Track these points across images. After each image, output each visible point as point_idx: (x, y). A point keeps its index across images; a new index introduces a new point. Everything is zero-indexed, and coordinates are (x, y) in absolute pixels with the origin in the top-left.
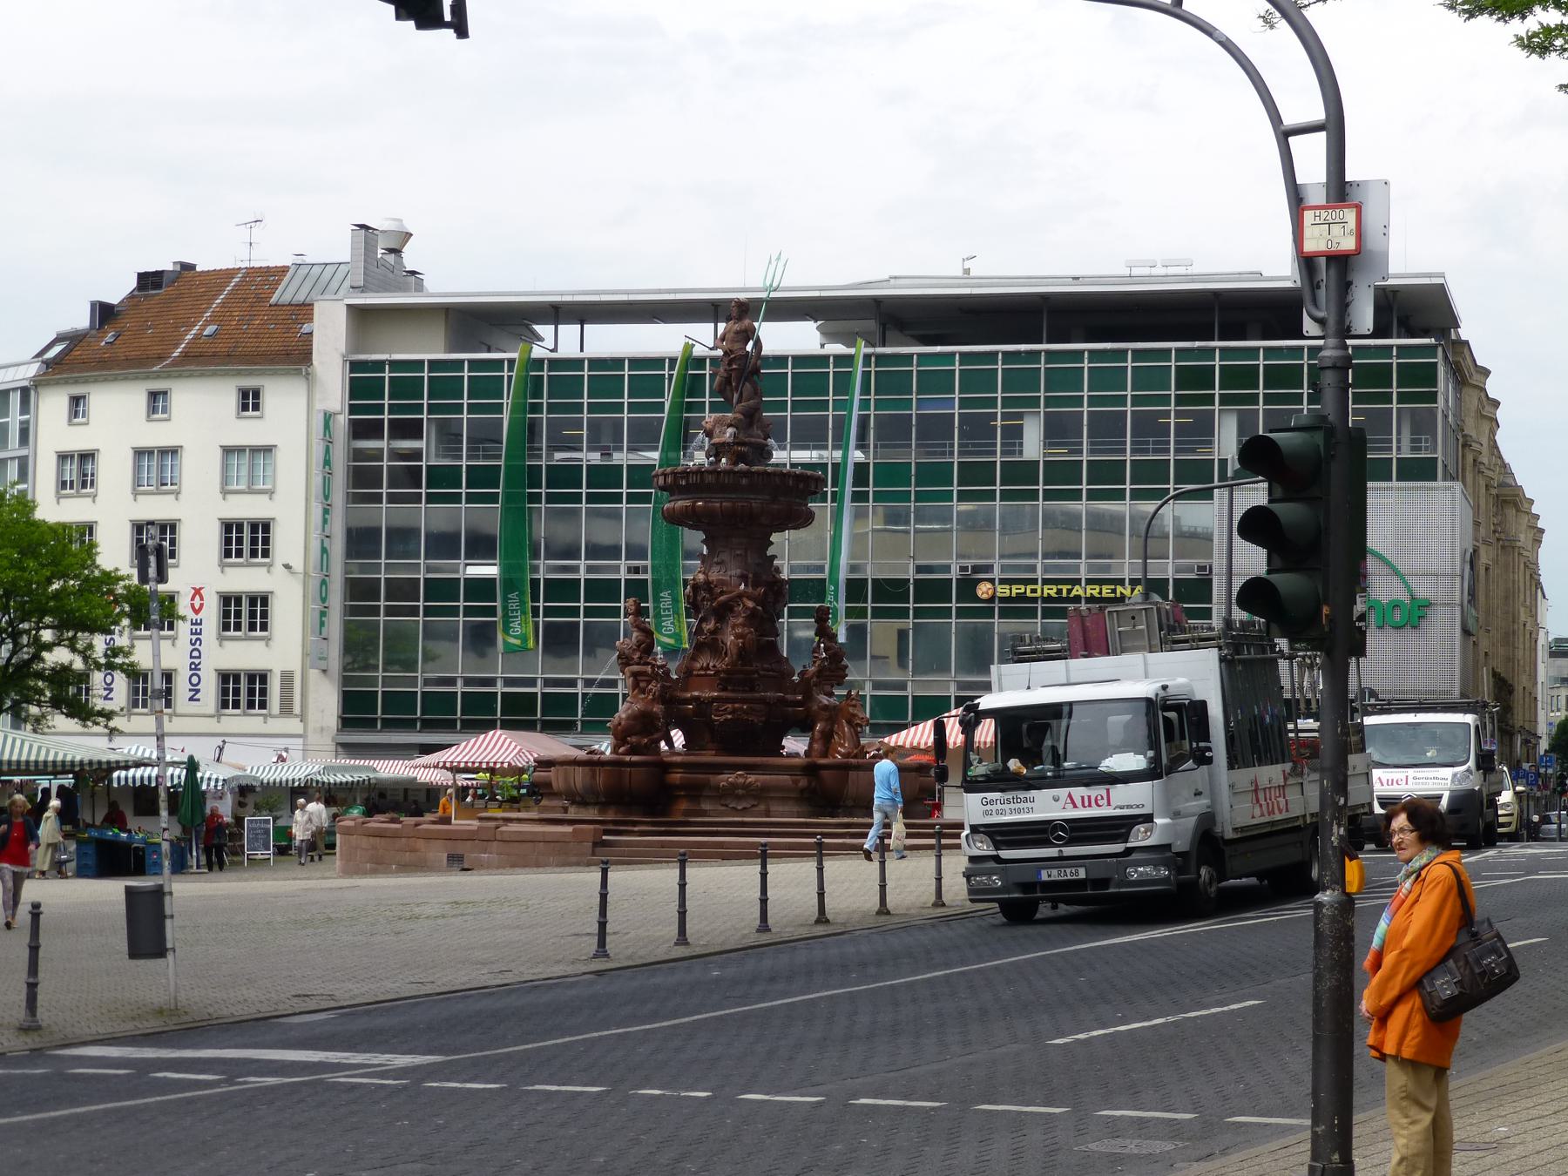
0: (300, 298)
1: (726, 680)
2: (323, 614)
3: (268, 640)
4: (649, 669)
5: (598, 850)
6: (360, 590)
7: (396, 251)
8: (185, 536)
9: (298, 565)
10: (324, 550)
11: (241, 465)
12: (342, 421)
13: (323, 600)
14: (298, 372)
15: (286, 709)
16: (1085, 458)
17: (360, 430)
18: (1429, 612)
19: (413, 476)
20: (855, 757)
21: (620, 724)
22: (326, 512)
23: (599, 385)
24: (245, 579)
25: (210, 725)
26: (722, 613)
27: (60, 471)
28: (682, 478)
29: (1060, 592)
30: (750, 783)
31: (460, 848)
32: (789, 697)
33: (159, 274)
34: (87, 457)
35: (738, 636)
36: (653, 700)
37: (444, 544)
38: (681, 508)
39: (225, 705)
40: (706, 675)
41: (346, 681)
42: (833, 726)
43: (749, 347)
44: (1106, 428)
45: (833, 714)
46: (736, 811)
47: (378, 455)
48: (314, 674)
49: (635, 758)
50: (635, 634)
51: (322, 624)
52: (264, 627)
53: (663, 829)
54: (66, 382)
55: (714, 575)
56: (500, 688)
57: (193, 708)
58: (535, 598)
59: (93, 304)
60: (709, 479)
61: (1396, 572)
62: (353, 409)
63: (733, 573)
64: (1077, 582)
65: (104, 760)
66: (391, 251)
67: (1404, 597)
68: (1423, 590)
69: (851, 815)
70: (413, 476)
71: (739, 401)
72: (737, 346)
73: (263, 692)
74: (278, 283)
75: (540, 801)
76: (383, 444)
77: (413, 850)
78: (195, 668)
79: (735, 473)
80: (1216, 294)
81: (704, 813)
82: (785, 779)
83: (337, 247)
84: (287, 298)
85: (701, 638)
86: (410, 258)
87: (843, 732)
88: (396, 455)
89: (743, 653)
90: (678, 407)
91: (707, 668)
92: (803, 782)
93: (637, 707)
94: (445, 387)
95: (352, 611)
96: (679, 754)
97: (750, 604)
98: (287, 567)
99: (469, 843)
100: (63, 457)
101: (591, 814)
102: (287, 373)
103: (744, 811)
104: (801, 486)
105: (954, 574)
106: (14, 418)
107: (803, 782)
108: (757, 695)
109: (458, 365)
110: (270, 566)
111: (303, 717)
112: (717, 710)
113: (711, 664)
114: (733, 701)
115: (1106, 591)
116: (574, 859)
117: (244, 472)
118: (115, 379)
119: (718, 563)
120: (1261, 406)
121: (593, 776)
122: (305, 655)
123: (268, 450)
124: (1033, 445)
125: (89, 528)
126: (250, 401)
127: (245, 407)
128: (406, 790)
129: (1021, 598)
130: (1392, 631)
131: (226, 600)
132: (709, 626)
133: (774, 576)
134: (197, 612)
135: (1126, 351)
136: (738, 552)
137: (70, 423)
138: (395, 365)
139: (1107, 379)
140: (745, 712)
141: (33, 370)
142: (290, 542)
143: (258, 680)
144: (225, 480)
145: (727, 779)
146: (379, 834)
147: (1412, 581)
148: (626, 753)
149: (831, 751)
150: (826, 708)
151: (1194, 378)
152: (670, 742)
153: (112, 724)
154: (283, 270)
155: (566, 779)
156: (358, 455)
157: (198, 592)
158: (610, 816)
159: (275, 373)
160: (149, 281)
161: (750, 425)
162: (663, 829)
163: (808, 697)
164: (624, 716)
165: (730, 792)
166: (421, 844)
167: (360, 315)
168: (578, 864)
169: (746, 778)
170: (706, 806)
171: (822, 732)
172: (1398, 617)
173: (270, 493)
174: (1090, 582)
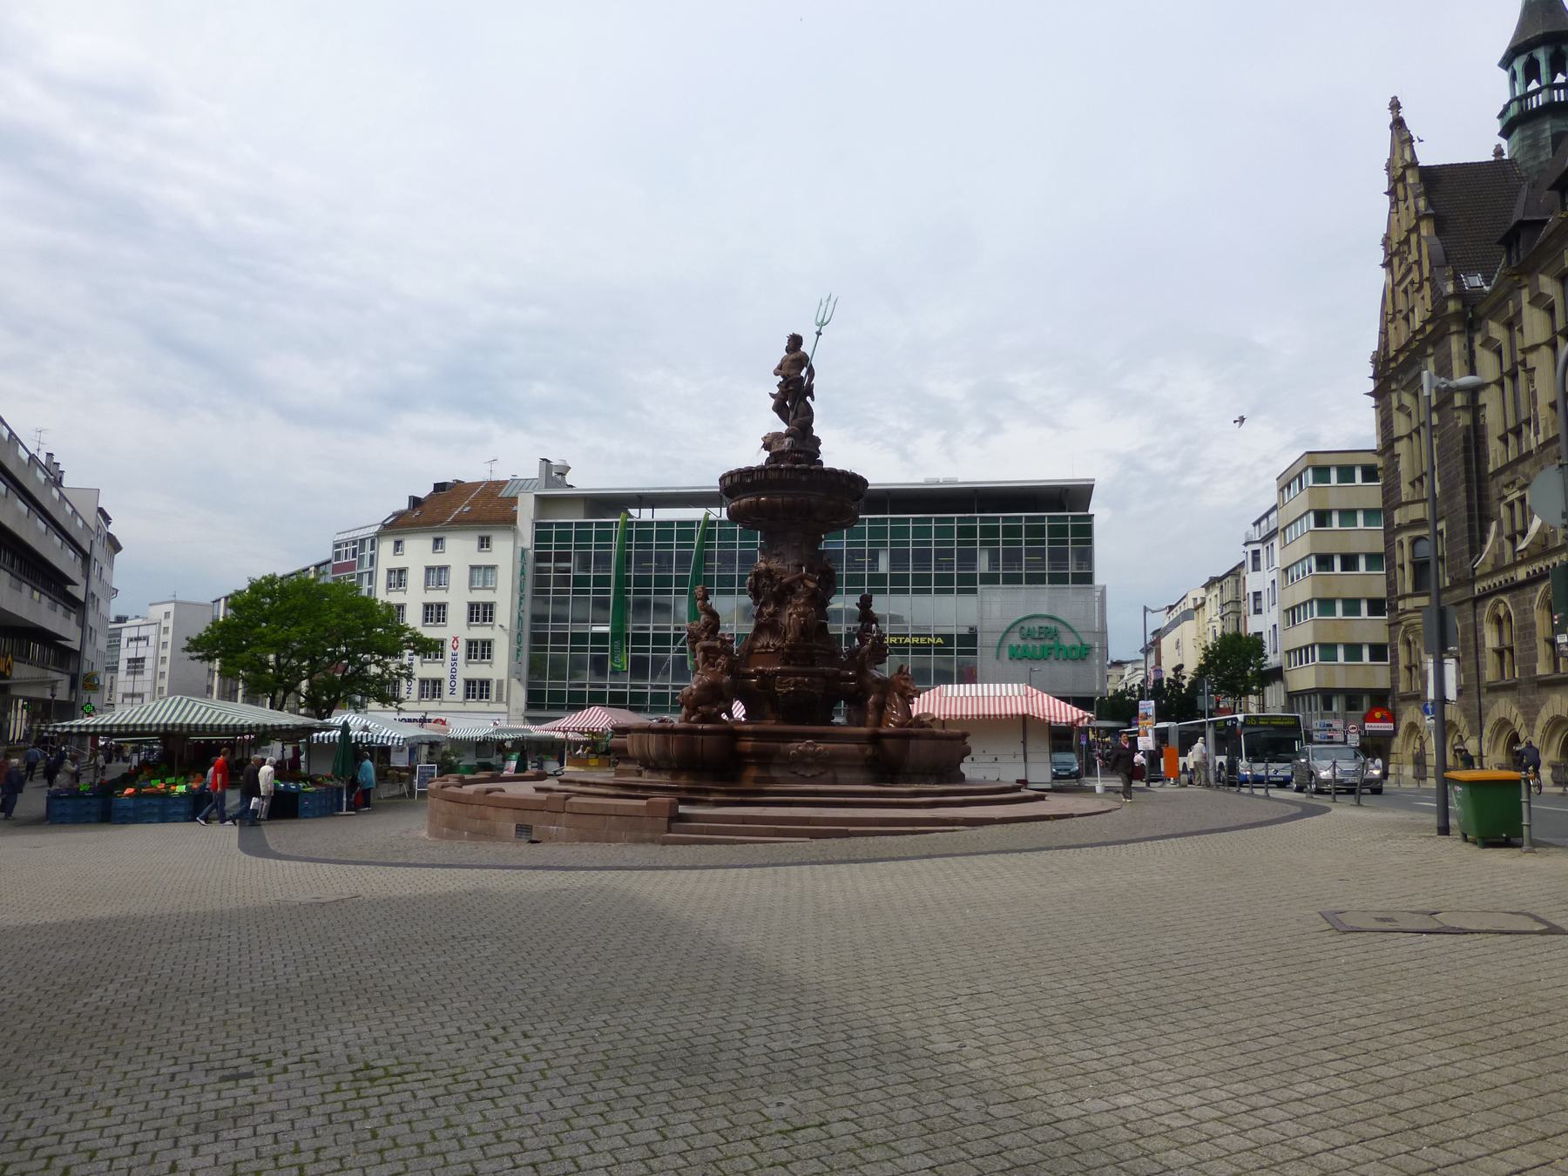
0: (513, 495)
1: (789, 656)
2: (518, 650)
3: (491, 664)
4: (718, 644)
5: (675, 825)
6: (538, 639)
7: (563, 475)
8: (450, 611)
9: (507, 625)
10: (520, 618)
11: (479, 576)
12: (531, 552)
13: (519, 643)
14: (509, 529)
15: (499, 699)
16: (911, 572)
17: (539, 558)
19: (566, 581)
20: (910, 726)
21: (691, 694)
22: (521, 598)
23: (660, 535)
24: (480, 633)
25: (461, 707)
26: (782, 595)
27: (389, 579)
28: (748, 476)
29: (898, 640)
30: (820, 751)
31: (529, 818)
32: (843, 673)
33: (444, 484)
34: (402, 571)
35: (799, 615)
36: (721, 672)
38: (746, 504)
39: (468, 697)
40: (767, 652)
41: (530, 684)
42: (885, 697)
43: (803, 373)
44: (922, 557)
45: (885, 686)
46: (805, 780)
48: (514, 681)
49: (707, 727)
50: (703, 617)
51: (518, 655)
52: (489, 657)
53: (739, 798)
54: (393, 534)
55: (774, 564)
56: (608, 689)
57: (452, 698)
58: (627, 644)
59: (410, 497)
60: (772, 475)
61: (1073, 631)
63: (791, 562)
64: (908, 635)
65: (269, 724)
66: (559, 474)
67: (1078, 644)
68: (1087, 642)
69: (910, 781)
70: (566, 581)
71: (794, 418)
72: (792, 372)
73: (488, 690)
74: (502, 488)
75: (617, 763)
76: (552, 565)
77: (484, 818)
78: (453, 677)
79: (796, 470)
80: (976, 490)
81: (774, 781)
82: (852, 747)
83: (533, 471)
84: (506, 495)
85: (762, 620)
86: (569, 479)
87: (895, 702)
88: (557, 570)
89: (804, 631)
90: (701, 545)
91: (768, 646)
92: (869, 751)
93: (707, 679)
94: (583, 536)
95: (532, 649)
96: (738, 722)
97: (812, 585)
98: (501, 626)
99: (538, 813)
100: (390, 571)
101: (662, 780)
102: (504, 529)
103: (812, 780)
104: (852, 486)
105: (843, 632)
106: (368, 552)
107: (869, 751)
108: (815, 669)
109: (590, 524)
110: (492, 626)
111: (508, 703)
112: (780, 683)
113: (771, 643)
114: (795, 674)
115: (922, 640)
116: (647, 835)
117: (481, 579)
118: (417, 532)
119: (776, 555)
120: (1001, 547)
121: (667, 744)
122: (509, 671)
123: (493, 568)
124: (884, 566)
125: (401, 607)
126: (484, 543)
127: (482, 546)
128: (553, 743)
130: (1071, 662)
131: (471, 644)
132: (771, 609)
133: (827, 566)
134: (455, 649)
135: (931, 518)
136: (796, 544)
137: (395, 554)
138: (559, 525)
139: (922, 532)
140: (806, 684)
141: (377, 528)
143: (485, 683)
144: (471, 581)
145: (796, 747)
146: (455, 799)
147: (1081, 635)
148: (699, 721)
149: (884, 721)
150: (878, 681)
151: (967, 532)
152: (730, 714)
153: (399, 706)
154: (506, 482)
155: (641, 747)
156: (539, 570)
157: (456, 639)
158: (683, 782)
159: (498, 529)
160: (439, 487)
161: (804, 438)
162: (739, 798)
163: (862, 671)
164: (695, 687)
165: (800, 760)
166: (490, 812)
167: (542, 501)
168: (652, 841)
169: (816, 747)
170: (776, 773)
171: (875, 703)
172: (1074, 654)
173: (494, 589)
174: (913, 635)
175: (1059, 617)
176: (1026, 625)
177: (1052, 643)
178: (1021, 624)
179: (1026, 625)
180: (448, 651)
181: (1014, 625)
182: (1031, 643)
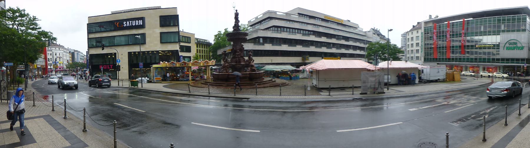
6: (425, 48)
12: (423, 33)
15: (420, 60)
17: (425, 34)
18: (524, 48)
37: (431, 44)
41: (424, 57)
47: (426, 36)
57: (414, 60)
62: (425, 32)
68: (523, 45)
95: (424, 51)
126: (418, 32)
129: (480, 47)
131: (417, 50)
142: (420, 45)
144: (416, 39)
175: (512, 39)
176: (510, 42)
177: (516, 46)
178: (508, 42)
179: (510, 42)
180: (414, 52)
181: (507, 42)
182: (511, 46)
